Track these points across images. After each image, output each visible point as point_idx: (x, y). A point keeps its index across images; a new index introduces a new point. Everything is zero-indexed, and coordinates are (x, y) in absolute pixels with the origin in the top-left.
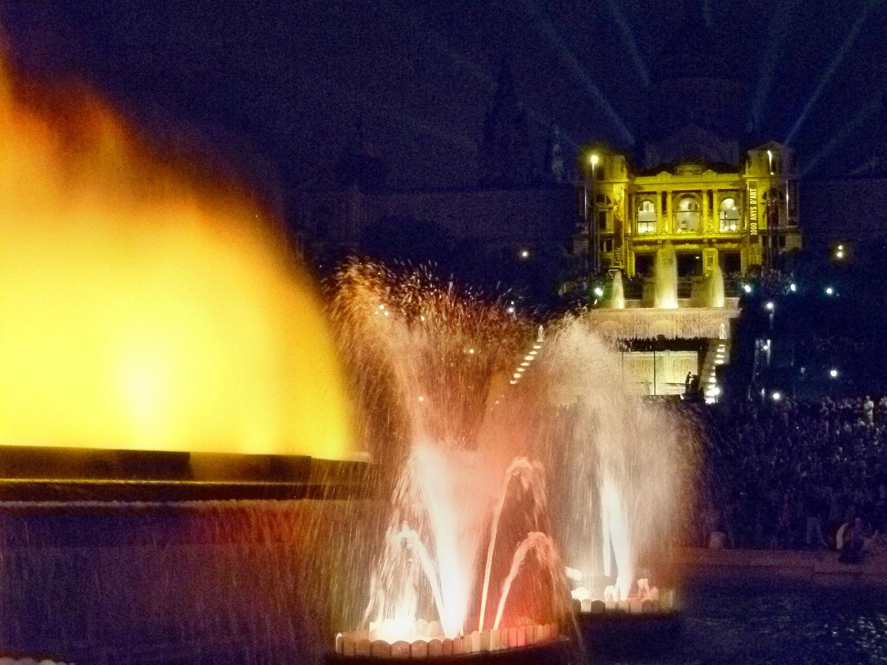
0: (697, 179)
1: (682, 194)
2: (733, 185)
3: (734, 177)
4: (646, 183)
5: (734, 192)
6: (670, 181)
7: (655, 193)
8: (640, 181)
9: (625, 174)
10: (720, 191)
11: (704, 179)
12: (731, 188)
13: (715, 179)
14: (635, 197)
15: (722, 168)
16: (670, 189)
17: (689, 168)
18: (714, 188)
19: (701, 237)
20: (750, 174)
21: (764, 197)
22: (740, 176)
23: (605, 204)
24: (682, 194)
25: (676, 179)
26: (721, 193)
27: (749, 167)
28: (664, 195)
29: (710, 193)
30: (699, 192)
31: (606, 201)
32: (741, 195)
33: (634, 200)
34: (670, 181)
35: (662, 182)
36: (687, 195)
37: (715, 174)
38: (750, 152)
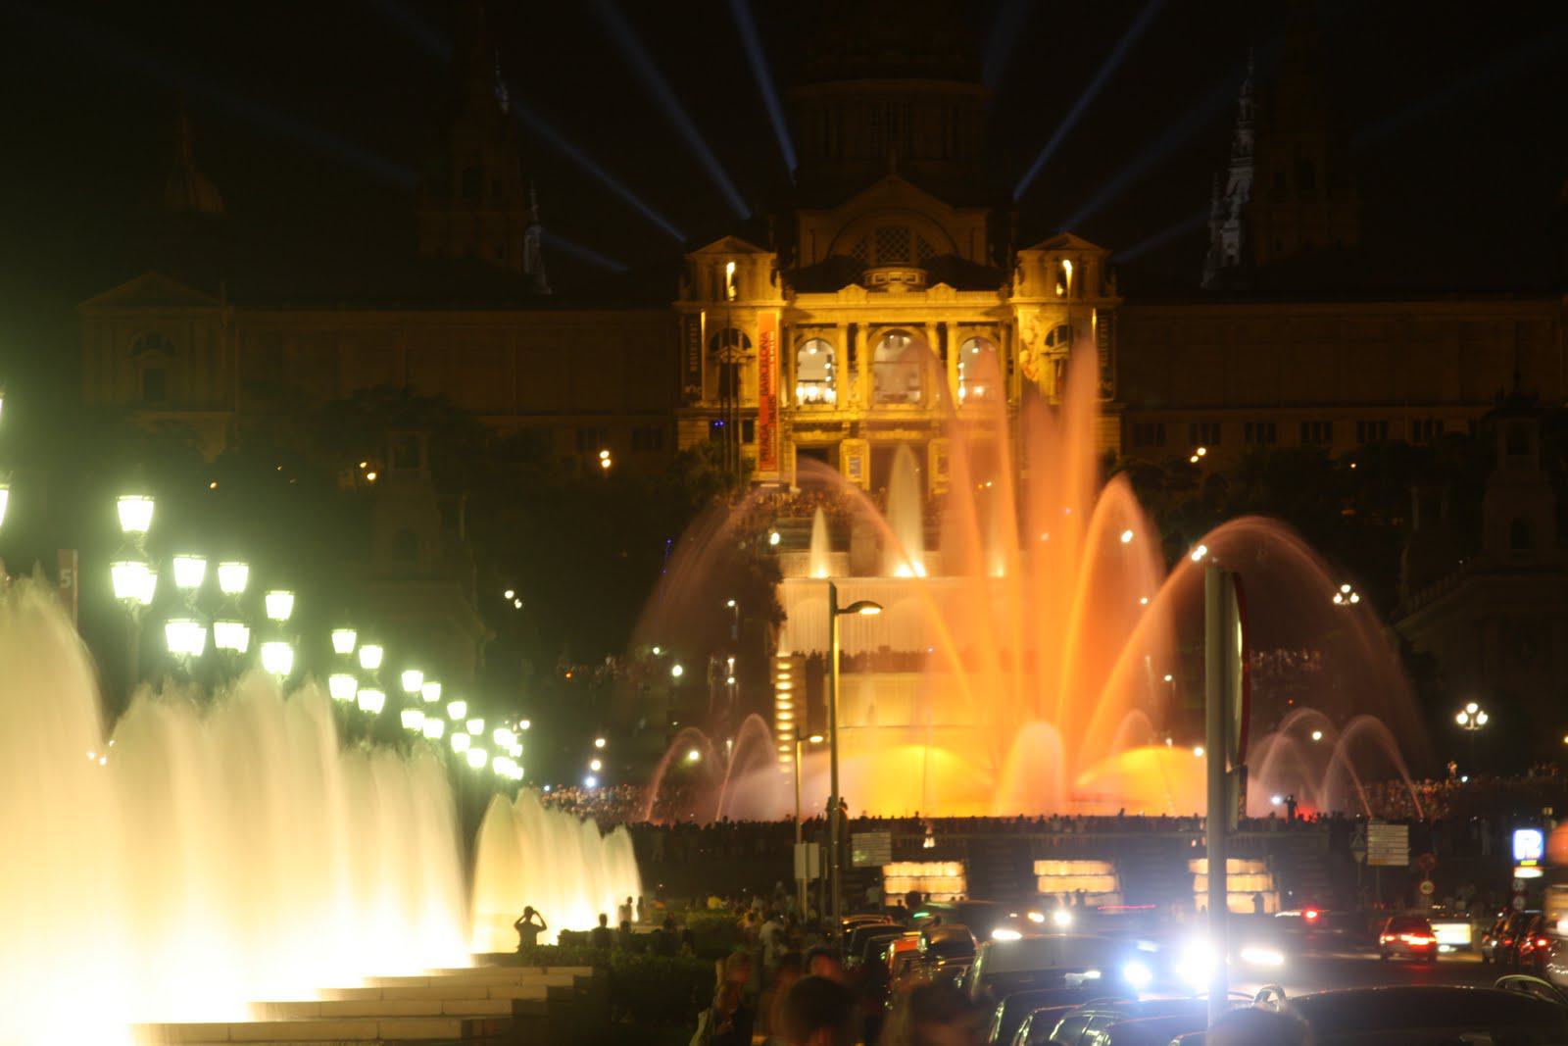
0: (918, 300)
1: (886, 329)
2: (987, 314)
3: (988, 300)
4: (817, 305)
5: (988, 329)
6: (863, 303)
7: (834, 326)
8: (807, 302)
9: (779, 291)
10: (961, 324)
11: (931, 302)
12: (983, 319)
13: (952, 302)
14: (794, 330)
15: (966, 278)
16: (863, 319)
17: (896, 273)
18: (951, 319)
19: (926, 417)
20: (1022, 294)
21: (1049, 341)
22: (1002, 297)
23: (740, 348)
24: (886, 329)
25: (877, 300)
26: (964, 329)
27: (1021, 283)
28: (853, 330)
29: (942, 329)
30: (920, 326)
31: (741, 343)
32: (1003, 334)
33: (792, 337)
34: (863, 303)
35: (847, 304)
36: (898, 329)
37: (952, 292)
38: (1021, 254)
